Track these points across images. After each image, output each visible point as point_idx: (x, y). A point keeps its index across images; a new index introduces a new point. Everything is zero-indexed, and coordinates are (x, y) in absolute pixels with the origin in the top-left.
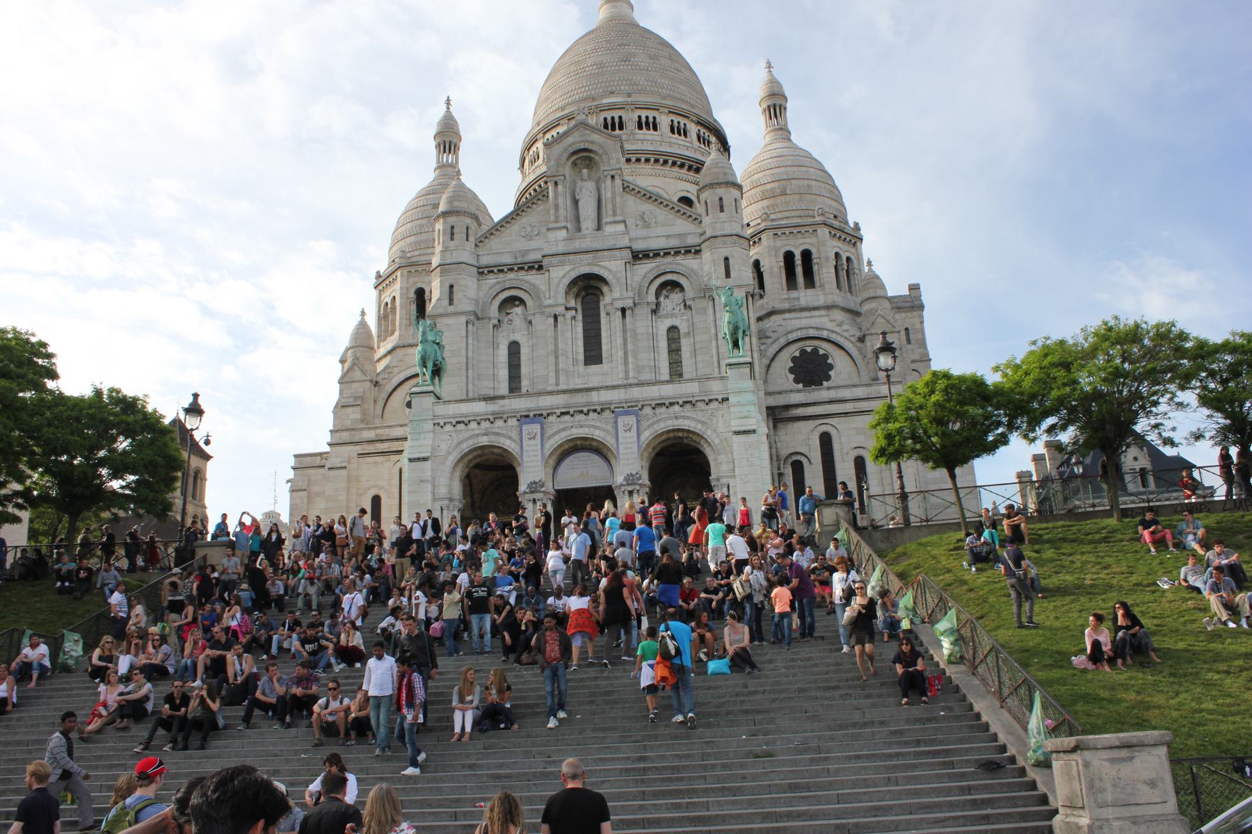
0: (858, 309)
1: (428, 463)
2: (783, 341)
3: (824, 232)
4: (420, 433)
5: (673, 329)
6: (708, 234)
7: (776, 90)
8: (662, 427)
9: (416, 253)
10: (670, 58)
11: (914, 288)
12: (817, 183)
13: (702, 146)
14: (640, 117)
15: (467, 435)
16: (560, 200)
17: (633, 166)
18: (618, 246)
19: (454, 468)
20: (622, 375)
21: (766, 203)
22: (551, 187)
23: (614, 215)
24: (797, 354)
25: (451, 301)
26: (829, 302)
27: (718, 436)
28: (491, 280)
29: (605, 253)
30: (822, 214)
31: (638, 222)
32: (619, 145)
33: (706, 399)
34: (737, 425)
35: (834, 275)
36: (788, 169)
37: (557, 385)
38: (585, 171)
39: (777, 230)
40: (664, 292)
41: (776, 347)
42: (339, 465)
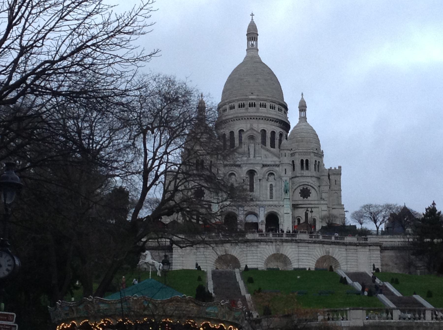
0: (319, 177)
2: (298, 185)
5: (271, 185)
6: (282, 162)
8: (269, 211)
13: (279, 112)
14: (261, 103)
21: (297, 144)
23: (259, 154)
24: (302, 189)
26: (312, 175)
31: (265, 157)
38: (252, 141)
39: (300, 153)
40: (270, 175)
41: (296, 187)
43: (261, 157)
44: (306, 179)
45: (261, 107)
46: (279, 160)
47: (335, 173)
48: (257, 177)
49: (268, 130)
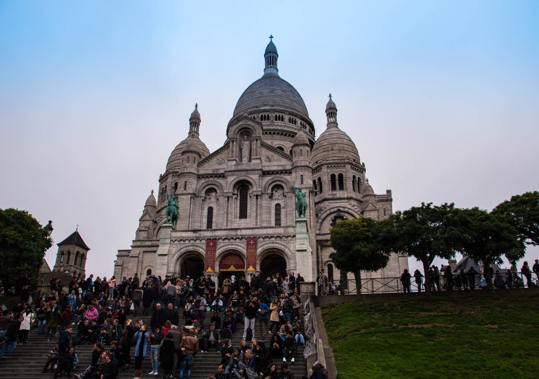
1: (167, 257)
2: (328, 212)
3: (348, 167)
4: (164, 244)
5: (278, 205)
6: (295, 165)
7: (332, 106)
9: (177, 168)
10: (291, 91)
11: (389, 192)
12: (347, 146)
14: (276, 115)
15: (184, 246)
16: (234, 149)
17: (272, 135)
18: (257, 169)
19: (178, 260)
20: (254, 224)
21: (325, 153)
22: (231, 143)
23: (256, 155)
25: (185, 189)
26: (349, 196)
27: (290, 251)
28: (203, 181)
29: (251, 172)
30: (348, 159)
32: (260, 126)
33: (286, 235)
34: (298, 247)
35: (352, 185)
36: (335, 139)
37: (227, 226)
38: (245, 137)
41: (325, 215)
42: (134, 256)
43: (260, 159)
44: (341, 202)
45: (276, 120)
46: (291, 164)
47: (382, 199)
48: (252, 193)
49: (286, 148)
